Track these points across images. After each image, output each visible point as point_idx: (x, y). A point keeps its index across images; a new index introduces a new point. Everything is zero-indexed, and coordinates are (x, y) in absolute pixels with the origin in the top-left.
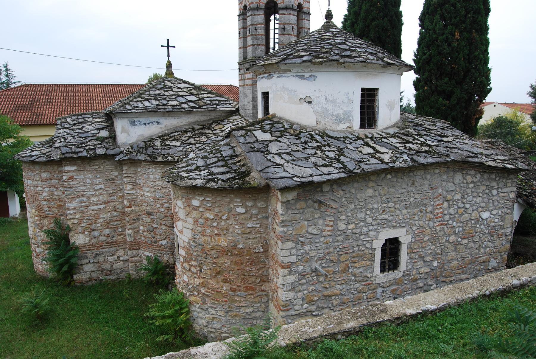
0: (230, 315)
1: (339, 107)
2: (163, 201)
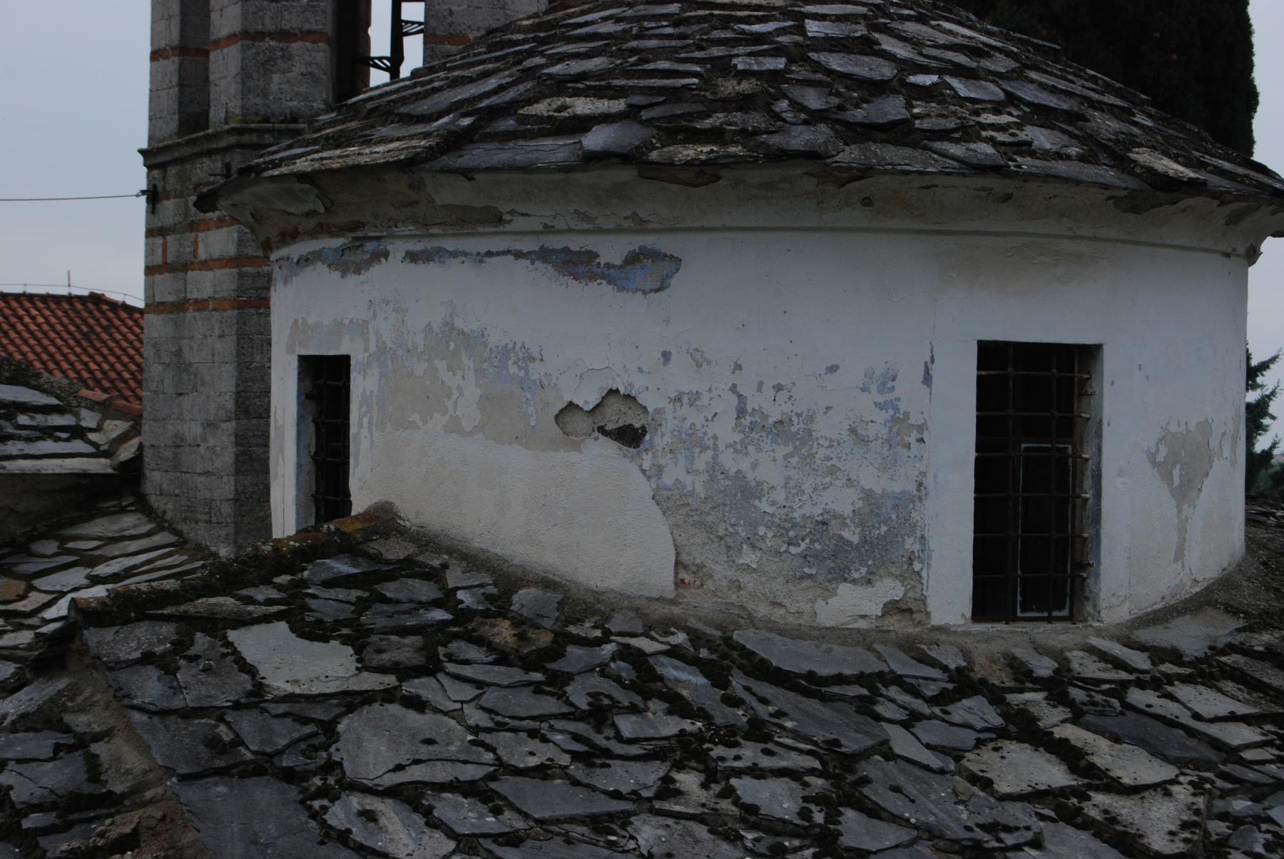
1: (832, 471)
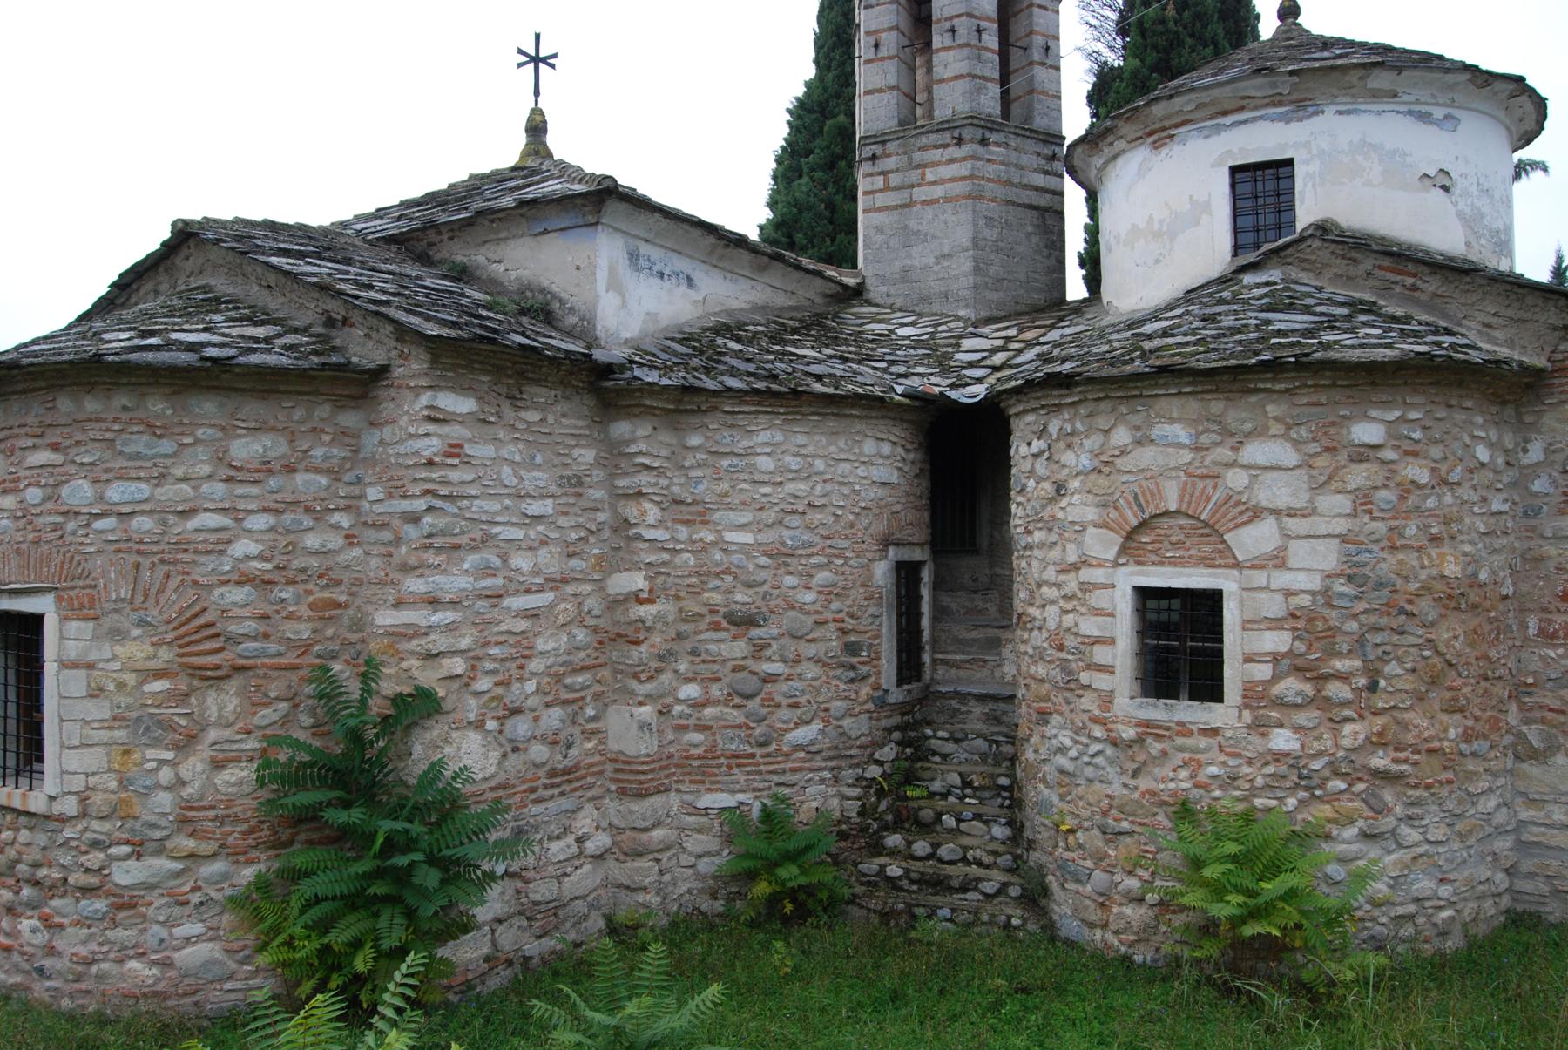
0: (1459, 834)
2: (813, 560)
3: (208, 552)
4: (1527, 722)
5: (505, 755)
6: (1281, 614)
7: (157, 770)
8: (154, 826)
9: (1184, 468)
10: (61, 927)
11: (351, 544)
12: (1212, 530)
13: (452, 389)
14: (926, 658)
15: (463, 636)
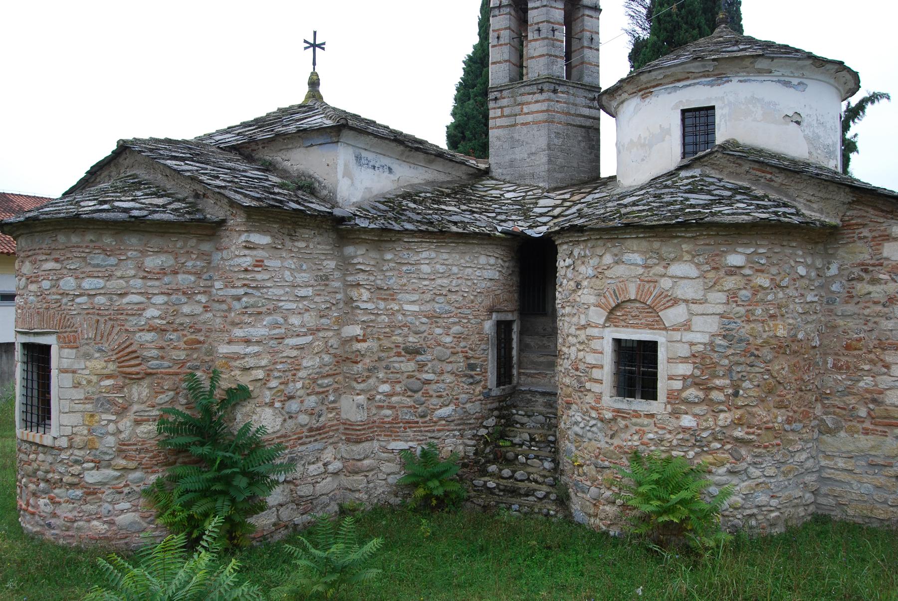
0: (783, 472)
3: (133, 315)
4: (826, 414)
5: (285, 420)
6: (688, 355)
7: (107, 425)
8: (106, 453)
9: (639, 277)
10: (59, 503)
11: (206, 311)
12: (652, 310)
13: (258, 232)
14: (515, 372)
15: (263, 359)
